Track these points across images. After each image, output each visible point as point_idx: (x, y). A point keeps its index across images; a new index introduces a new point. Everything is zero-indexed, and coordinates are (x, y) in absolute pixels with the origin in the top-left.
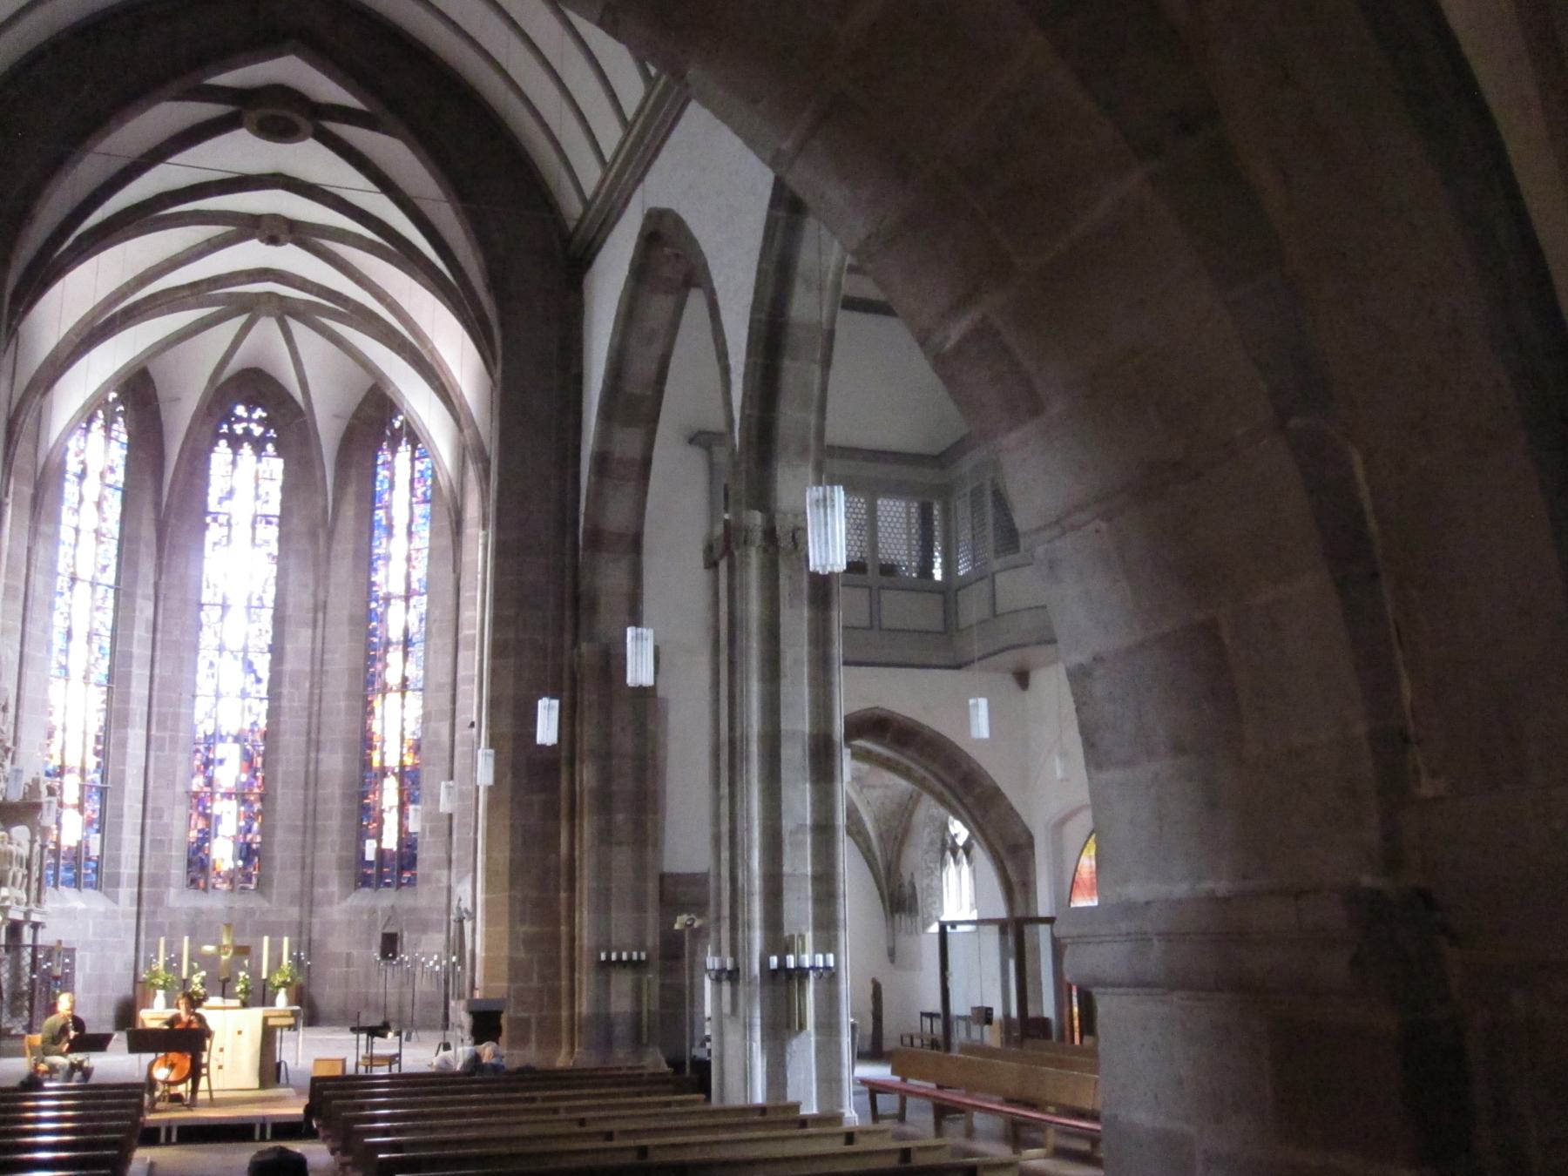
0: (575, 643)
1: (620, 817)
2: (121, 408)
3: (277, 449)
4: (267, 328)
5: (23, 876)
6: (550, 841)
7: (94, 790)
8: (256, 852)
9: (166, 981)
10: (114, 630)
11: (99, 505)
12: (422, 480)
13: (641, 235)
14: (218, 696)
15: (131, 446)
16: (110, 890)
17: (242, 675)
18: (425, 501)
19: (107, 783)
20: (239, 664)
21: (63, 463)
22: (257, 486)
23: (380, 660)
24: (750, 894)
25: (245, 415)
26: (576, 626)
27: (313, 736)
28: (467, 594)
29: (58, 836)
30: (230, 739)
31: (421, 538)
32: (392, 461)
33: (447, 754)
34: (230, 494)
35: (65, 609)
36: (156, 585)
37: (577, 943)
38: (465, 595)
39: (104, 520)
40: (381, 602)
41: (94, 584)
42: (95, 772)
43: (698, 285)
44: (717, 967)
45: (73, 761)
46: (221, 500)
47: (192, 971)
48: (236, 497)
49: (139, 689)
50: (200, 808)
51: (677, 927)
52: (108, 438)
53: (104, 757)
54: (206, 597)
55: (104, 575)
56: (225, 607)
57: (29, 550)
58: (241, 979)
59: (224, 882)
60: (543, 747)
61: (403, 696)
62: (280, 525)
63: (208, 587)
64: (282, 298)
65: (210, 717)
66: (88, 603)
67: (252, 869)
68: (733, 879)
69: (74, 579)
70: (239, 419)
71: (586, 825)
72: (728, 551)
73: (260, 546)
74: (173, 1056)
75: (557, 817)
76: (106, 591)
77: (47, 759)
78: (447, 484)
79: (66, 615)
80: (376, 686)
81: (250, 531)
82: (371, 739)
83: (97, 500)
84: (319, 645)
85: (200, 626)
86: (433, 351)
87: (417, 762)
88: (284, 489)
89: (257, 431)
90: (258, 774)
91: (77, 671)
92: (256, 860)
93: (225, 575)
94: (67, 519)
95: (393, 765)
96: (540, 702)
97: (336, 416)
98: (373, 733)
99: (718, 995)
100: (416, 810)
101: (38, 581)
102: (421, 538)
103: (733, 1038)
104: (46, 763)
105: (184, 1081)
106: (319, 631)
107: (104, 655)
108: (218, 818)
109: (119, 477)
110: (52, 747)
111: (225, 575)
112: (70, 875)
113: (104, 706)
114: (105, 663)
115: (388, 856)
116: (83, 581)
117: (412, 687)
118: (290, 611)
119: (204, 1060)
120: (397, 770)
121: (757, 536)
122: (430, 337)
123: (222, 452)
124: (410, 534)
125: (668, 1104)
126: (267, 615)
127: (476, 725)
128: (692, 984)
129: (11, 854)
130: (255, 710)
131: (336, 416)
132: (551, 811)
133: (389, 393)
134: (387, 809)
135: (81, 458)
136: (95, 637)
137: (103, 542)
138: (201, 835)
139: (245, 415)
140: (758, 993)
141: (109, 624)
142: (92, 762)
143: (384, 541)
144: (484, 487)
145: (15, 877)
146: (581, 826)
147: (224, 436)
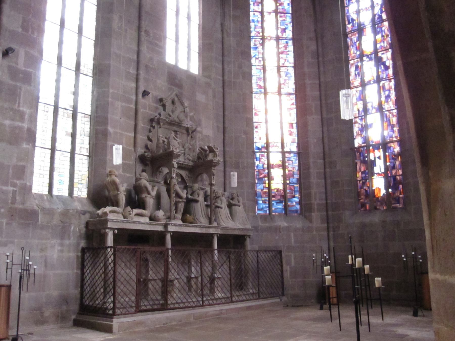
8: (400, 182)
16: (307, 214)
20: (372, 63)
29: (269, 184)
30: (374, 110)
41: (278, 39)
50: (362, 158)
55: (284, 34)
56: (360, 30)
57: (222, 25)
59: (382, 204)
67: (399, 194)
76: (287, 43)
85: (347, 48)
90: (395, 129)
91: (272, 86)
92: (401, 186)
108: (373, 163)
130: (387, 87)
138: (364, 175)
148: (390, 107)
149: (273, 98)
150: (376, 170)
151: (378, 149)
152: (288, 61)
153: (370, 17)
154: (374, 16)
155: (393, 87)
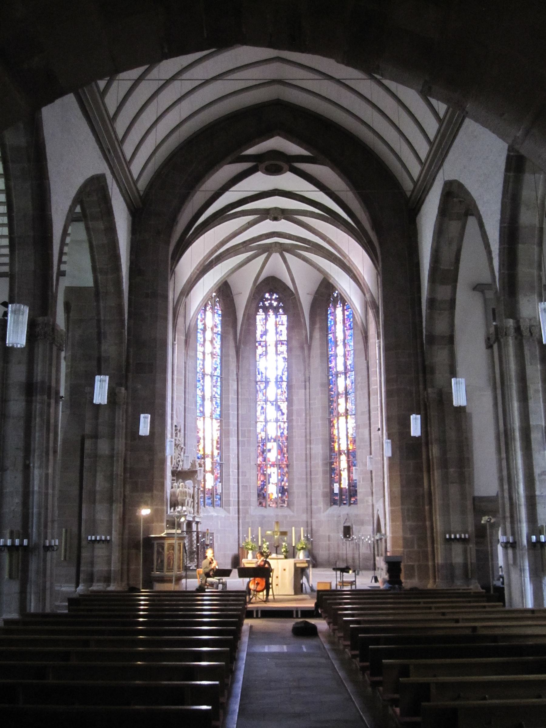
0: (425, 389)
1: (452, 470)
2: (218, 299)
3: (284, 311)
4: (276, 257)
5: (192, 502)
6: (419, 481)
7: (217, 464)
8: (286, 490)
9: (252, 547)
10: (221, 395)
11: (212, 342)
12: (348, 319)
13: (442, 194)
14: (266, 421)
15: (223, 316)
16: (226, 507)
17: (275, 412)
18: (350, 329)
19: (222, 461)
20: (274, 407)
21: (196, 324)
22: (277, 328)
23: (335, 402)
24: (520, 505)
25: (269, 297)
26: (425, 381)
27: (308, 438)
28: (372, 370)
29: (205, 484)
30: (272, 440)
31: (349, 346)
32: (335, 312)
33: (368, 444)
34: (265, 333)
35: (201, 387)
36: (237, 375)
37: (435, 530)
38: (372, 370)
39: (214, 348)
40: (334, 376)
41: (212, 376)
42: (217, 456)
43: (472, 215)
44: (505, 541)
45: (208, 452)
46: (261, 336)
47: (263, 542)
48: (268, 334)
49: (233, 420)
51: (483, 522)
52: (213, 313)
53: (220, 450)
54: (259, 378)
56: (267, 382)
57: (185, 363)
58: (284, 546)
59: (273, 504)
60: (415, 437)
61: (347, 418)
62: (287, 345)
63: (259, 374)
64: (281, 244)
65: (263, 431)
66: (210, 384)
67: (285, 498)
68: (511, 498)
69: (204, 375)
70: (267, 299)
71: (436, 474)
72: (497, 340)
73: (279, 355)
74: (258, 580)
75: (421, 471)
76: (217, 379)
77: (198, 452)
78: (360, 320)
79: (201, 390)
80: (334, 414)
81: (275, 348)
82: (334, 438)
83: (210, 340)
84: (308, 397)
86: (349, 260)
87: (354, 447)
88: (288, 329)
89: (275, 304)
91: (208, 412)
92: (286, 493)
93: (266, 369)
94: (200, 349)
95: (344, 449)
96: (411, 416)
97: (308, 294)
98: (334, 435)
99: (506, 555)
100: (356, 469)
101: (190, 376)
102: (349, 346)
103: (514, 576)
104: (198, 454)
105: (262, 591)
106: (308, 390)
107: (218, 406)
108: (270, 475)
109: (219, 329)
110: (200, 446)
111: (266, 369)
112: (210, 501)
113: (219, 428)
114: (219, 409)
115: (344, 490)
116: (207, 375)
117: (350, 413)
118: (294, 382)
119: (270, 582)
120: (346, 452)
121: (512, 331)
122: (347, 253)
123: (260, 316)
124: (345, 345)
125: (484, 607)
126: (284, 384)
127: (380, 429)
128: (492, 550)
129: (186, 492)
130: (282, 427)
131: (308, 294)
132: (418, 468)
133: (330, 281)
134: (342, 470)
135: (203, 322)
136: (214, 399)
137: (214, 358)
138: (262, 483)
139: (269, 297)
140: (527, 554)
141: (219, 392)
142: (216, 452)
143: (333, 348)
144: (377, 319)
145: (188, 502)
146: (433, 474)
147: (261, 307)
148: (283, 441)
149: (208, 420)
150: (271, 480)
151: (274, 467)
152: (217, 394)
153: (275, 376)
154: (277, 375)
155: (286, 428)
